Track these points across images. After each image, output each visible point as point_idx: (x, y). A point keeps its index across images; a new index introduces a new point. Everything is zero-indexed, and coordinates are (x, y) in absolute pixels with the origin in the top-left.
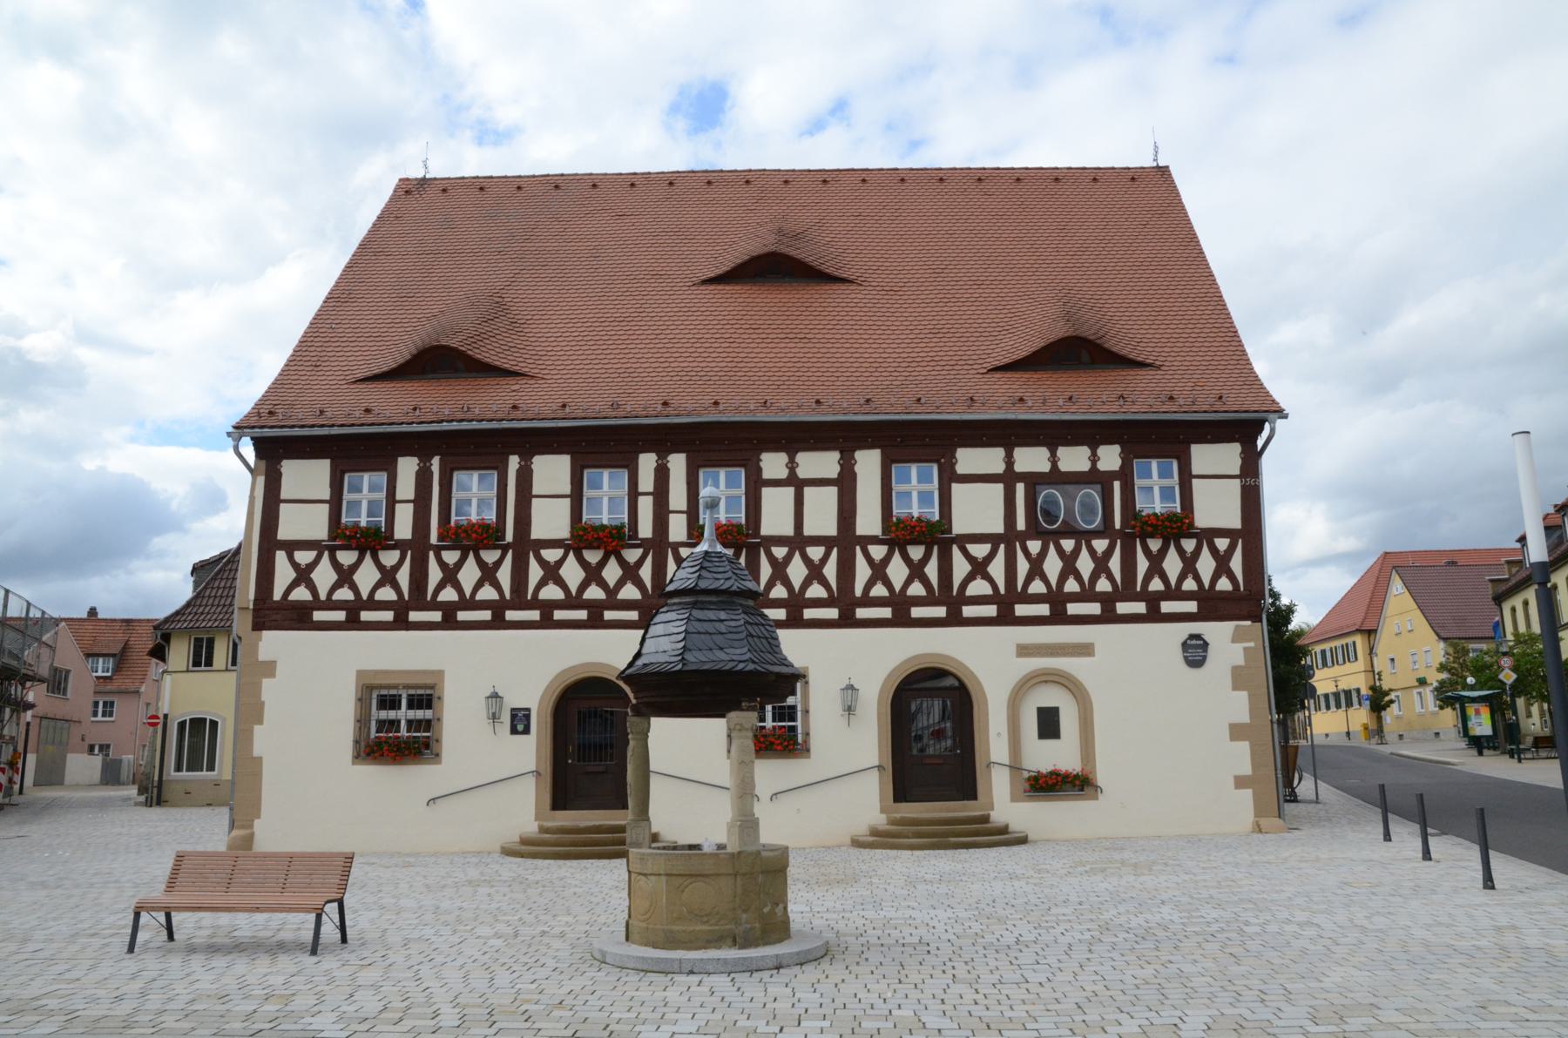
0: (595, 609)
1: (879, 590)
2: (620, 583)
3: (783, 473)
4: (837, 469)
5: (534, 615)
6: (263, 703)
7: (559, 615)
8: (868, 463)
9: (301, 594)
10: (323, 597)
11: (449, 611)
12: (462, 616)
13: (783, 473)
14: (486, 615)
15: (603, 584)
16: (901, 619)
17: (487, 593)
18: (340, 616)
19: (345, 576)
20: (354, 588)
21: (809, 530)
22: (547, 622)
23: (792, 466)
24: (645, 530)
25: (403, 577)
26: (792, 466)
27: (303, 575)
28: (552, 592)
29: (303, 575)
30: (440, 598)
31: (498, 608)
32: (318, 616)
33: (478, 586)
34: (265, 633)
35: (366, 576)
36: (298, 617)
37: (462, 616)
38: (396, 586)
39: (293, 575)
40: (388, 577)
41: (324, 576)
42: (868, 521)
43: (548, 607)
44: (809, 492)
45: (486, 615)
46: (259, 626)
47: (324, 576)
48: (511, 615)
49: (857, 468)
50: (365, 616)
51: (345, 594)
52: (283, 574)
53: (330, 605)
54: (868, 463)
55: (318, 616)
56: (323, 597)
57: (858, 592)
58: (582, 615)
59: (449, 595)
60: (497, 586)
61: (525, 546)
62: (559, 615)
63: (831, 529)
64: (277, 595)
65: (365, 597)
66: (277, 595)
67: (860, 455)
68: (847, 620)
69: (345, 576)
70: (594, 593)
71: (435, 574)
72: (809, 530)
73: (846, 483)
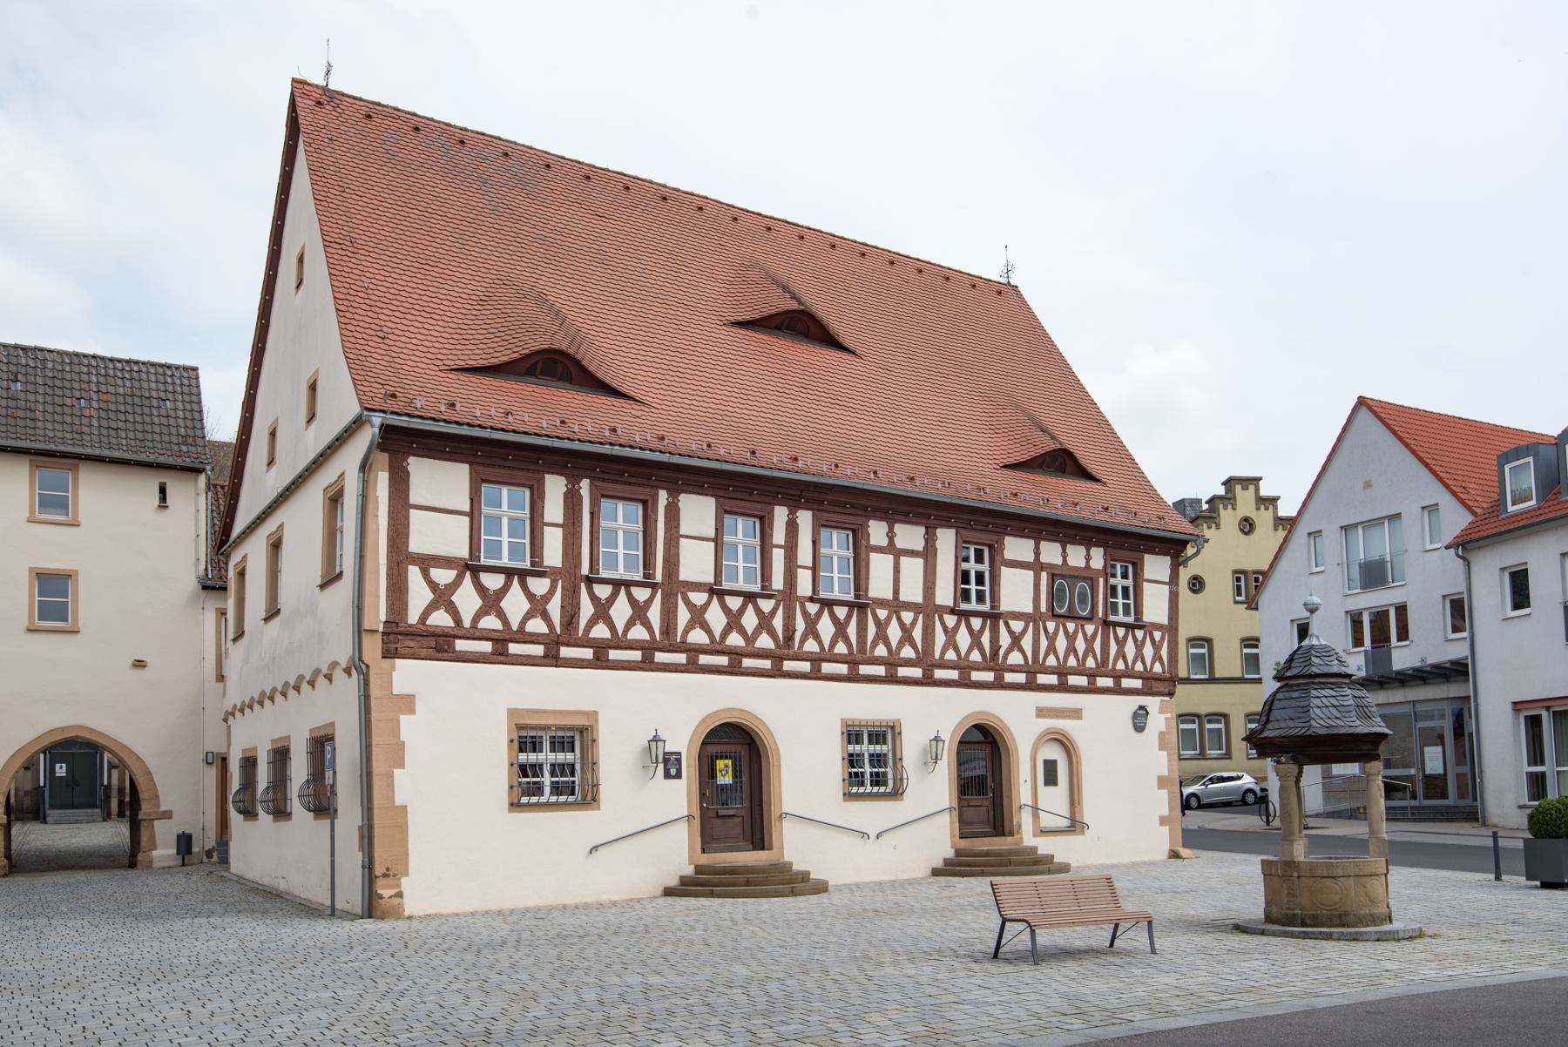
0: (736, 654)
1: (951, 655)
2: (757, 633)
3: (884, 542)
4: (923, 543)
5: (681, 658)
6: (402, 746)
7: (704, 659)
8: (946, 539)
9: (440, 619)
10: (467, 623)
11: (601, 648)
12: (614, 655)
13: (884, 542)
14: (636, 655)
15: (742, 632)
16: (965, 683)
17: (639, 633)
18: (486, 647)
19: (492, 602)
20: (502, 616)
21: (902, 598)
22: (692, 667)
23: (891, 535)
24: (778, 582)
25: (555, 607)
26: (891, 535)
27: (442, 597)
28: (698, 637)
29: (442, 597)
31: (648, 648)
32: (461, 645)
33: (630, 624)
35: (515, 604)
36: (439, 646)
37: (614, 655)
38: (546, 617)
39: (429, 596)
40: (538, 606)
41: (467, 600)
42: (945, 594)
43: (694, 651)
44: (904, 560)
45: (636, 655)
46: (389, 654)
47: (467, 600)
48: (660, 657)
49: (938, 544)
51: (490, 622)
52: (419, 595)
53: (475, 634)
54: (946, 539)
55: (461, 645)
56: (467, 623)
57: (937, 656)
58: (723, 660)
59: (600, 631)
60: (647, 625)
61: (673, 588)
62: (704, 659)
63: (918, 598)
64: (413, 617)
66: (413, 617)
67: (939, 531)
68: (928, 681)
69: (492, 602)
70: (735, 640)
71: (587, 609)
72: (902, 598)
73: (928, 554)
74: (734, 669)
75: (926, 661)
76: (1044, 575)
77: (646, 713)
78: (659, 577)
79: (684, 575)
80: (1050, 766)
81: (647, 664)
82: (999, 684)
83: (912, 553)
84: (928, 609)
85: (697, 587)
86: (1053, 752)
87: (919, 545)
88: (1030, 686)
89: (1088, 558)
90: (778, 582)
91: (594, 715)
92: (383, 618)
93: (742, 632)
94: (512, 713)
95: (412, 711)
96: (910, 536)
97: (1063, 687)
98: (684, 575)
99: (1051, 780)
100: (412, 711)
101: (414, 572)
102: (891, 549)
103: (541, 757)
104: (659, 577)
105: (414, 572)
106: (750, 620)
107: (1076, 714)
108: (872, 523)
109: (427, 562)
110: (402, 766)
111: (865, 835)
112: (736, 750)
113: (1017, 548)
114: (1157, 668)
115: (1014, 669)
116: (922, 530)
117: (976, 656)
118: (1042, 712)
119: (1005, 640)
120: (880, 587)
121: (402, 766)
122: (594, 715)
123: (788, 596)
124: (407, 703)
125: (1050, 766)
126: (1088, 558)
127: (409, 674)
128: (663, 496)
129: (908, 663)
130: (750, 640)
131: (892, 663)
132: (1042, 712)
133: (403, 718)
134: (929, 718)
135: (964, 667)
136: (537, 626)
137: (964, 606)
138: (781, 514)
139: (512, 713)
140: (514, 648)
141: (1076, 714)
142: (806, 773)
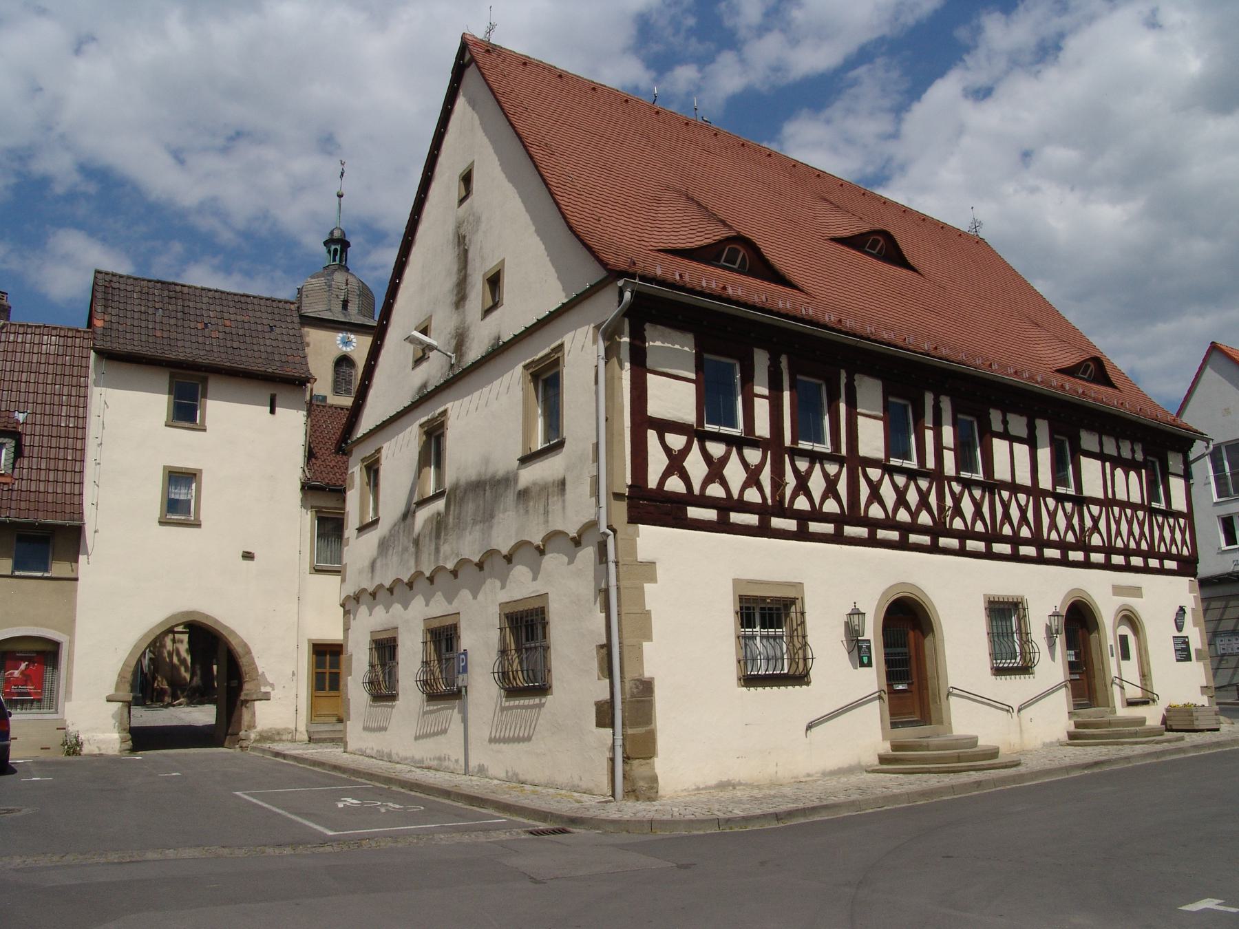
0: (905, 529)
5: (863, 532)
6: (649, 612)
9: (675, 484)
11: (802, 518)
16: (1064, 562)
18: (711, 514)
19: (716, 470)
24: (930, 464)
27: (676, 464)
28: (876, 512)
29: (676, 464)
30: (796, 507)
32: (693, 512)
34: (642, 528)
41: (696, 466)
43: (873, 524)
46: (637, 517)
47: (696, 466)
50: (735, 517)
53: (704, 501)
54: (1042, 428)
55: (693, 512)
56: (697, 491)
58: (894, 535)
62: (882, 534)
63: (1028, 483)
64: (652, 483)
65: (736, 496)
68: (1040, 560)
69: (716, 470)
74: (903, 545)
75: (1039, 541)
76: (1108, 464)
77: (841, 584)
78: (844, 452)
79: (864, 451)
80: (1124, 640)
81: (838, 538)
82: (1087, 564)
83: (1021, 440)
84: (1034, 491)
85: (874, 463)
86: (1125, 630)
87: (1024, 433)
88: (1108, 566)
89: (1133, 451)
90: (930, 464)
91: (800, 585)
92: (629, 482)
93: (908, 508)
94: (737, 582)
95: (653, 579)
96: (1018, 425)
97: (1128, 568)
98: (864, 451)
99: (1125, 655)
100: (653, 579)
101: (652, 435)
102: (1005, 435)
103: (758, 629)
104: (844, 452)
105: (652, 435)
106: (912, 497)
107: (1136, 592)
108: (991, 411)
109: (664, 427)
110: (650, 639)
111: (1008, 709)
112: (907, 620)
113: (1089, 441)
114: (1185, 552)
115: (1097, 549)
116: (1024, 420)
117: (1070, 537)
118: (1118, 590)
119: (1088, 523)
120: (1001, 472)
121: (650, 639)
122: (800, 585)
123: (937, 476)
124: (648, 570)
125: (1124, 640)
126: (1133, 451)
127: (652, 540)
128: (843, 375)
129: (1026, 542)
130: (914, 515)
131: (1016, 541)
132: (1118, 590)
133: (647, 586)
134: (1044, 590)
135: (1063, 546)
136: (752, 495)
137: (1060, 490)
138: (929, 399)
139: (737, 582)
140: (735, 517)
141: (1136, 592)
142: (962, 648)
